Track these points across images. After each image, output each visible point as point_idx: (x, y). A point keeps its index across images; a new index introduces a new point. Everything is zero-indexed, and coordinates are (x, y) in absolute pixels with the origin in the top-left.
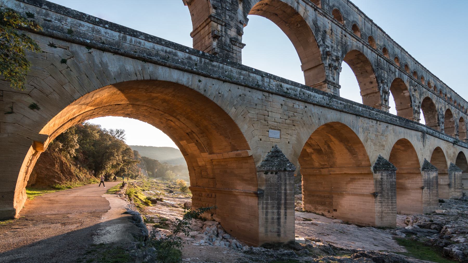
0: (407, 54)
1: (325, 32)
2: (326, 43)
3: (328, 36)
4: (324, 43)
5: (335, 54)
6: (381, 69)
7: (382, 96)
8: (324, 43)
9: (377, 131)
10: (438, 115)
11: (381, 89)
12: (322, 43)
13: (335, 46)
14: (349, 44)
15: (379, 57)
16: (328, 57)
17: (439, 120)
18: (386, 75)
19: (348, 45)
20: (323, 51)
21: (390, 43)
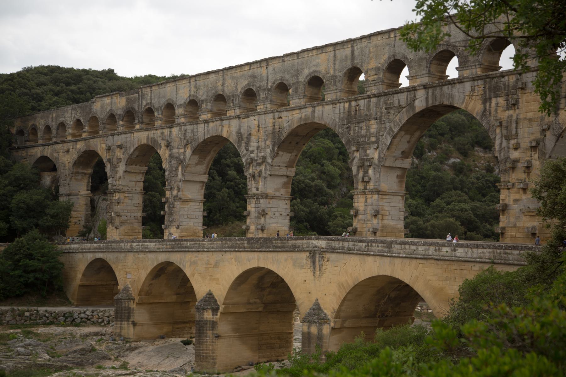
1: (250, 135)
2: (251, 149)
3: (253, 138)
5: (262, 154)
6: (359, 123)
8: (247, 150)
9: (208, 263)
12: (245, 151)
15: (353, 103)
18: (374, 127)
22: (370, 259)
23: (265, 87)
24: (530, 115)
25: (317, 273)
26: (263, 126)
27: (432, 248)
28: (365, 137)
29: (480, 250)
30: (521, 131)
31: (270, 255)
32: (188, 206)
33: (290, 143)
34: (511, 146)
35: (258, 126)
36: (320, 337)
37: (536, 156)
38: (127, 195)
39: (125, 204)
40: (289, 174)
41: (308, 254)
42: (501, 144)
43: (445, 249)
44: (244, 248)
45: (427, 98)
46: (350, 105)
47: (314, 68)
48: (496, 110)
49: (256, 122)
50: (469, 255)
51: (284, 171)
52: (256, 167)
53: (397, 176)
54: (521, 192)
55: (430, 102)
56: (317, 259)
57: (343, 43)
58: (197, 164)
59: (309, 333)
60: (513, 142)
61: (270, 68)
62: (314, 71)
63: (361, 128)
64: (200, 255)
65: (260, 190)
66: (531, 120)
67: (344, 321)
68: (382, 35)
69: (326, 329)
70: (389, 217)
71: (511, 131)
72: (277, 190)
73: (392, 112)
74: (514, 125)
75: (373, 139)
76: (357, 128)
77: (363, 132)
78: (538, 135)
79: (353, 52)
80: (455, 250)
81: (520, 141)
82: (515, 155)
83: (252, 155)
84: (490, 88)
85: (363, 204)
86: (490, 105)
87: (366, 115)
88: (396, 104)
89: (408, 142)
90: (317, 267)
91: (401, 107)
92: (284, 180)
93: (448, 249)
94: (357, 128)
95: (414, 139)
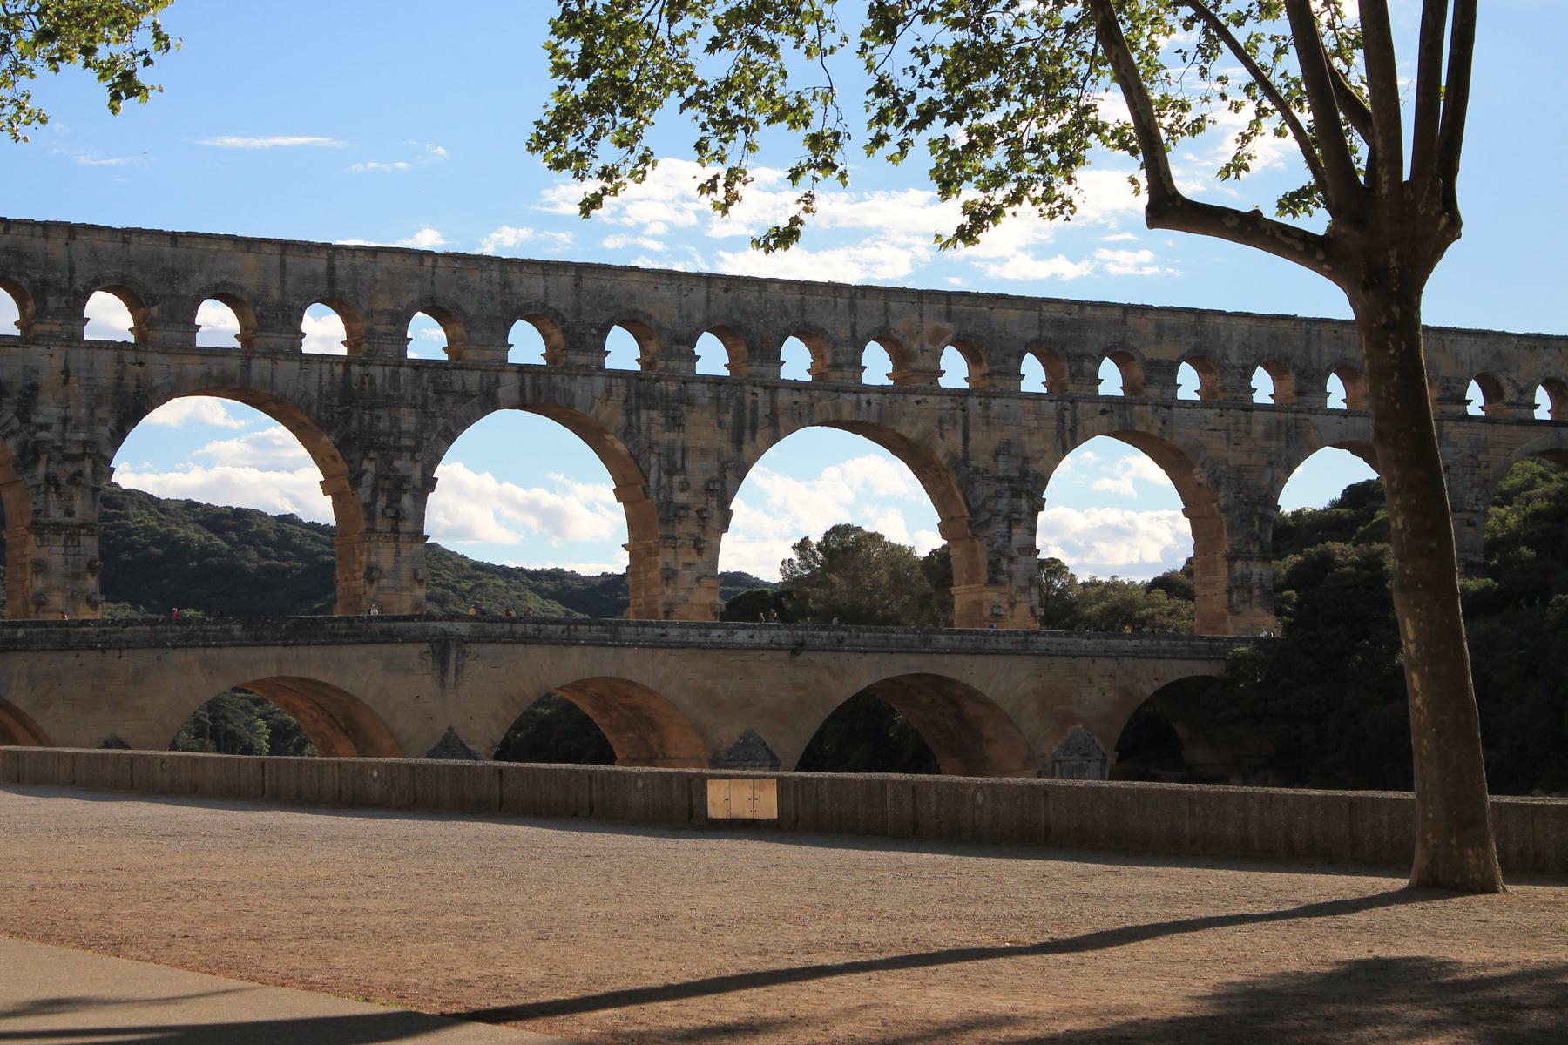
0: (636, 276)
1: (35, 388)
4: (25, 420)
5: (82, 436)
7: (369, 507)
8: (25, 420)
10: (966, 485)
11: (367, 480)
12: (16, 423)
13: (83, 412)
14: (158, 382)
15: (356, 370)
16: (44, 458)
17: (974, 512)
18: (409, 420)
19: (153, 390)
20: (23, 448)
21: (474, 277)
22: (574, 651)
23: (65, 285)
24: (702, 443)
25: (450, 679)
26: (83, 374)
27: (693, 632)
28: (389, 435)
29: (773, 633)
30: (689, 465)
31: (316, 652)
34: (676, 485)
35: (66, 372)
37: (714, 503)
41: (425, 647)
42: (659, 480)
43: (715, 633)
44: (233, 638)
45: (522, 389)
46: (347, 371)
47: (224, 278)
48: (649, 429)
49: (58, 363)
50: (756, 640)
52: (61, 463)
54: (694, 552)
55: (529, 395)
56: (453, 656)
57: (307, 248)
60: (677, 479)
61: (81, 245)
62: (224, 284)
63: (379, 418)
64: (70, 658)
65: (78, 515)
66: (703, 452)
71: (674, 463)
73: (449, 400)
74: (679, 455)
75: (407, 442)
76: (367, 418)
77: (383, 425)
78: (716, 475)
79: (331, 269)
80: (733, 634)
81: (689, 479)
82: (681, 498)
83: (43, 435)
84: (639, 395)
85: (391, 560)
86: (638, 416)
87: (389, 396)
88: (458, 386)
90: (452, 669)
91: (465, 396)
93: (722, 632)
94: (367, 418)
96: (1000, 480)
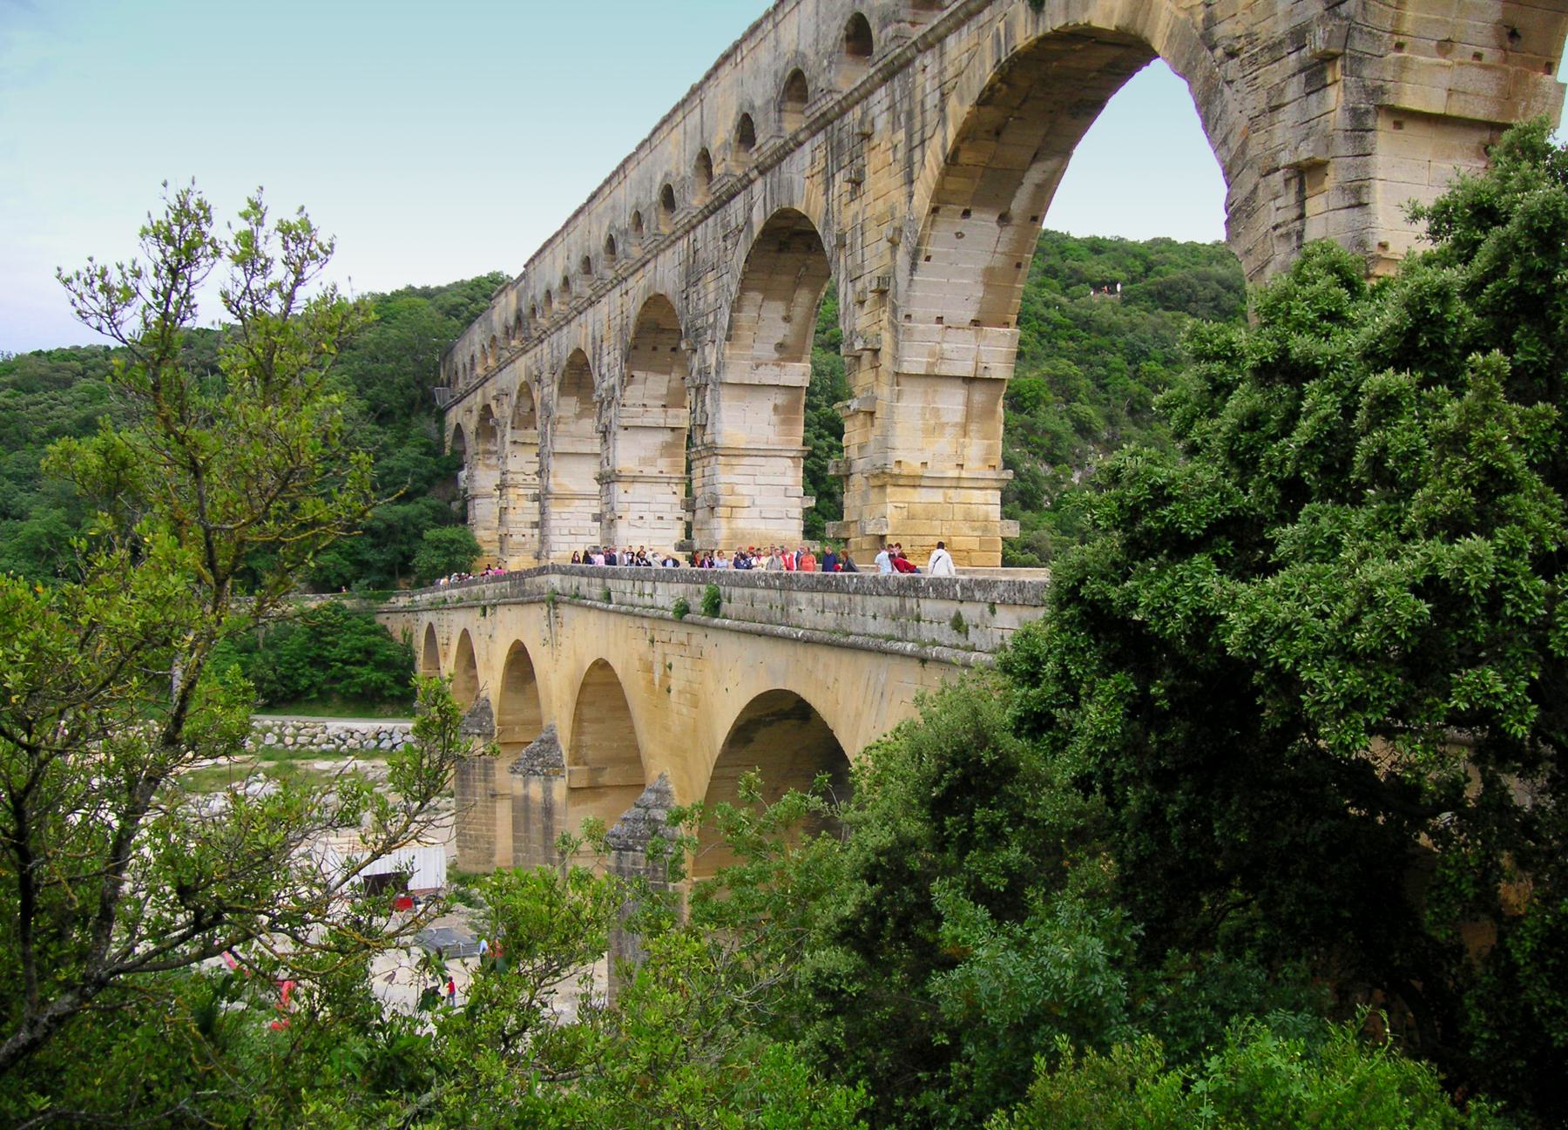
32: (571, 509)
33: (655, 349)
36: (548, 810)
38: (522, 491)
39: (519, 511)
40: (672, 423)
51: (656, 417)
53: (776, 408)
58: (579, 416)
59: (526, 798)
67: (596, 771)
68: (732, 60)
69: (559, 789)
70: (755, 512)
72: (644, 461)
89: (787, 319)
92: (667, 436)
95: (798, 312)
96: (1274, 50)
